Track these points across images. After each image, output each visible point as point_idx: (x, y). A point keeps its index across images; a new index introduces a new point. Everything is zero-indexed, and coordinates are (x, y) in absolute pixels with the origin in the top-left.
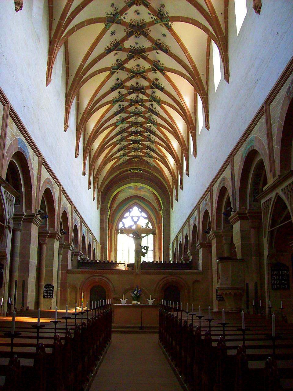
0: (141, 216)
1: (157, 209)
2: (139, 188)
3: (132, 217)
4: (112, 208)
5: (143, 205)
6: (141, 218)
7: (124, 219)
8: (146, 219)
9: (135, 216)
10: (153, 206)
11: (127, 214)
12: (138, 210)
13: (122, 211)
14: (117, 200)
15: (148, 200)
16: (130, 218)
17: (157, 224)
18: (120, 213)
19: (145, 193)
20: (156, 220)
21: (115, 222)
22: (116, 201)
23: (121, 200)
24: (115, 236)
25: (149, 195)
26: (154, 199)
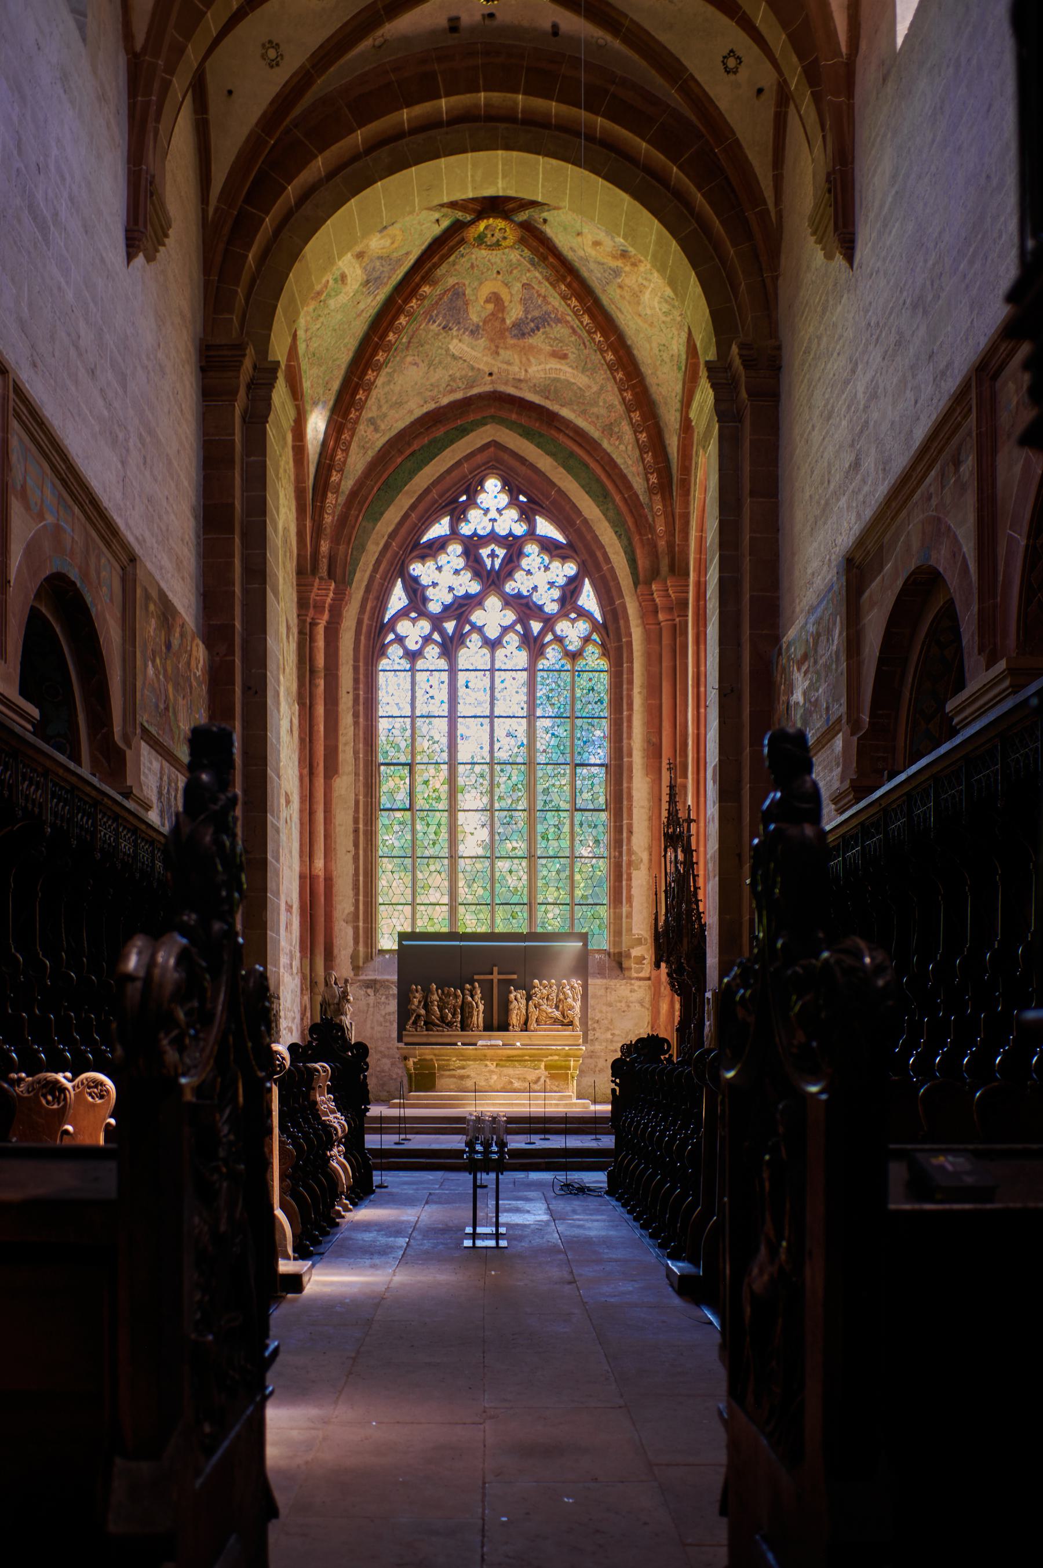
0: (531, 534)
1: (638, 484)
2: (515, 325)
3: (472, 546)
4: (335, 477)
5: (545, 463)
6: (532, 556)
7: (423, 558)
8: (564, 558)
9: (493, 537)
10: (610, 465)
11: (440, 528)
12: (504, 499)
13: (403, 502)
14: (367, 414)
15: (581, 423)
16: (455, 549)
17: (636, 583)
18: (392, 516)
19: (554, 364)
20: (632, 562)
21: (358, 575)
22: (362, 428)
23: (399, 420)
24: (356, 669)
25: (581, 380)
26: (620, 408)
